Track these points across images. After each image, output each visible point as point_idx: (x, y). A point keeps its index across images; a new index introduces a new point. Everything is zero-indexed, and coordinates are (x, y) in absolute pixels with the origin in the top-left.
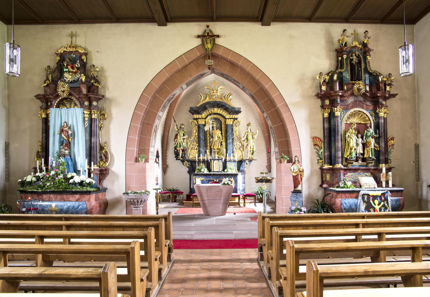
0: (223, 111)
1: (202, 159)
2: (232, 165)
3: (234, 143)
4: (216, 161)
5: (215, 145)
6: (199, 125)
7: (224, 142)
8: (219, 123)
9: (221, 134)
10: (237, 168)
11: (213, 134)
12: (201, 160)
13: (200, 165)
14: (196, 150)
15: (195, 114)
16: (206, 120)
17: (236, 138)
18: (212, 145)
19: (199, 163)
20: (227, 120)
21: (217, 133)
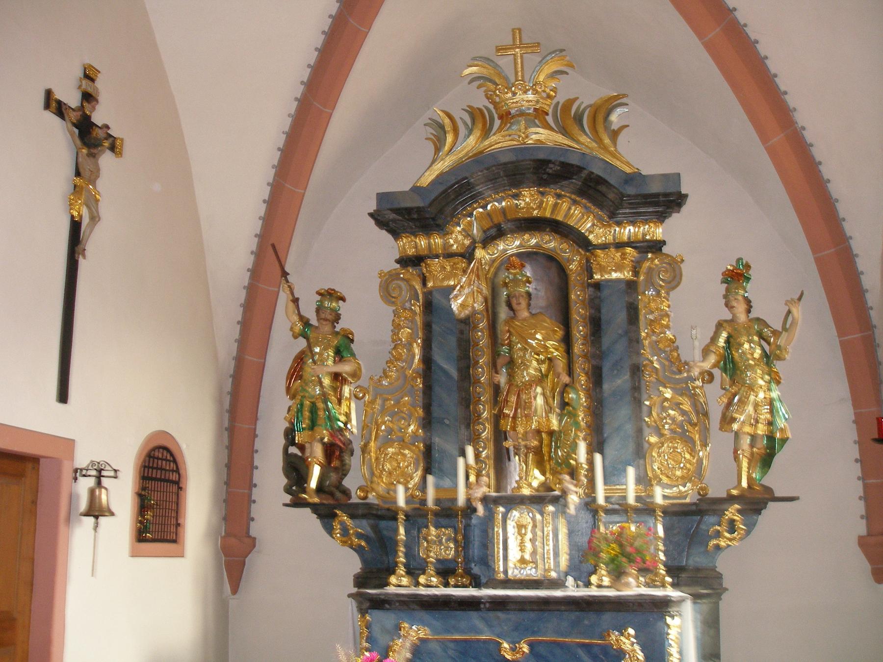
0: (575, 202)
15: (405, 231)
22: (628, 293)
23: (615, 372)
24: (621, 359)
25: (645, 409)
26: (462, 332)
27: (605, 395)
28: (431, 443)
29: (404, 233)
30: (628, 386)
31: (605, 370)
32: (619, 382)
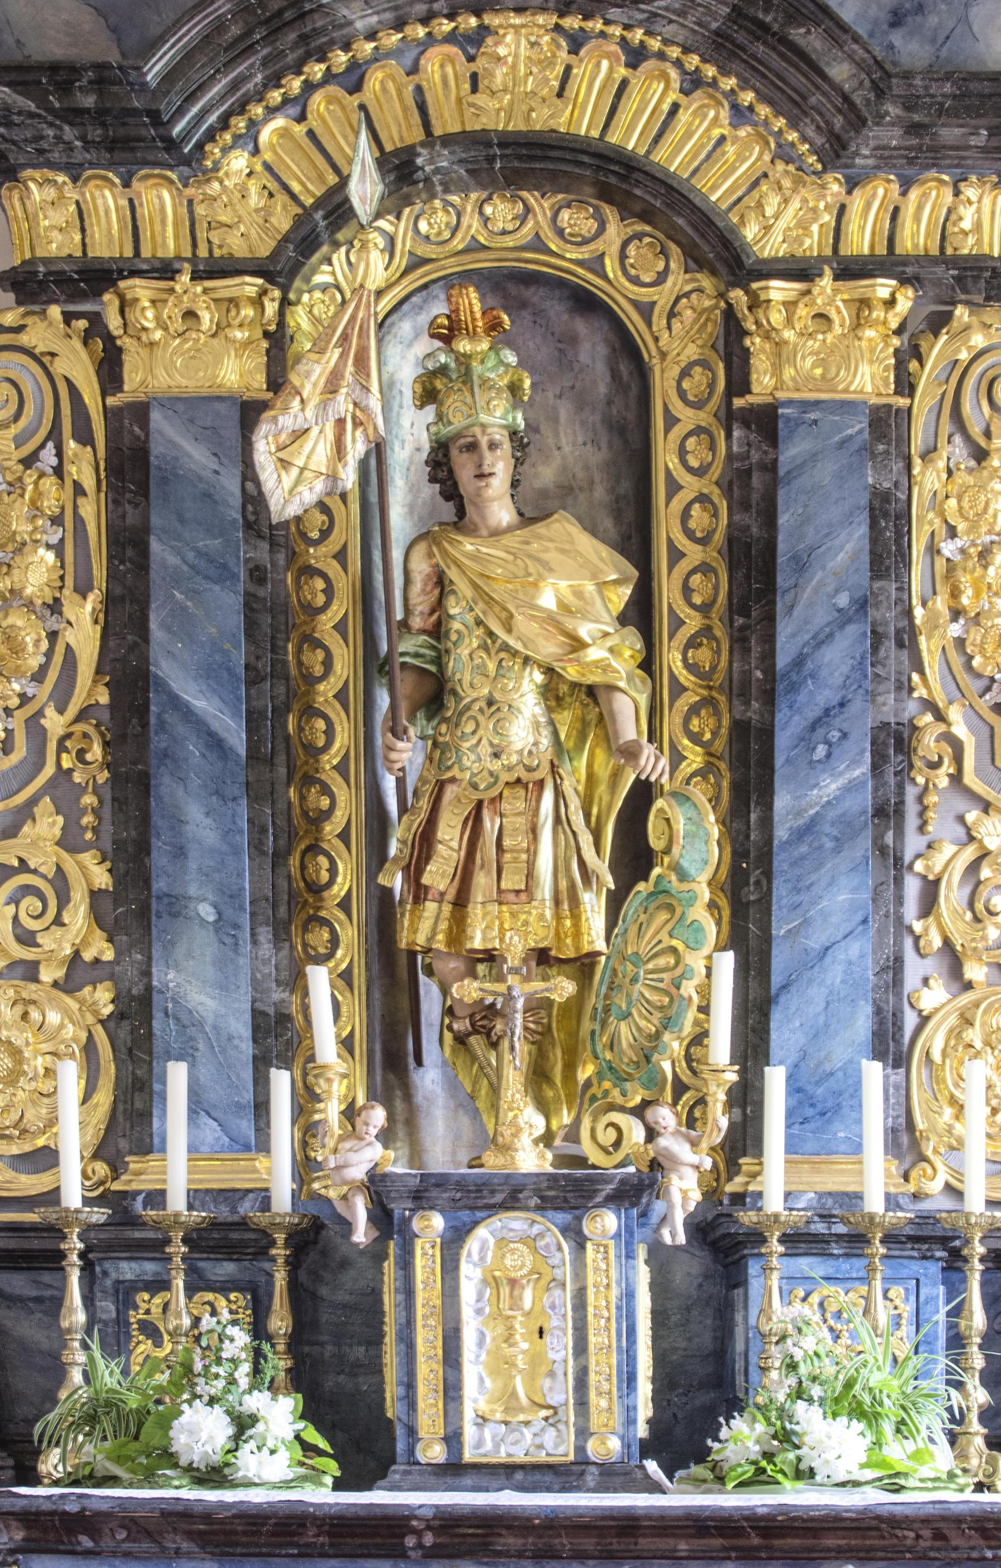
0: (693, 83)
1: (195, 1198)
2: (883, 1315)
3: (913, 843)
4: (515, 1222)
5: (482, 881)
6: (140, 411)
7: (699, 793)
8: (581, 403)
9: (623, 620)
10: (980, 1396)
11: (438, 631)
12: (177, 1202)
13: (151, 1331)
14: (67, 986)
15: (42, 160)
16: (300, 318)
17: (960, 730)
18: (414, 871)
19: (128, 1270)
20: (778, 290)
21: (547, 600)
22: (873, 456)
23: (821, 750)
24: (842, 705)
25: (912, 887)
26: (257, 574)
27: (781, 833)
28: (149, 988)
29: (35, 166)
30: (865, 800)
31: (783, 740)
32: (830, 786)
